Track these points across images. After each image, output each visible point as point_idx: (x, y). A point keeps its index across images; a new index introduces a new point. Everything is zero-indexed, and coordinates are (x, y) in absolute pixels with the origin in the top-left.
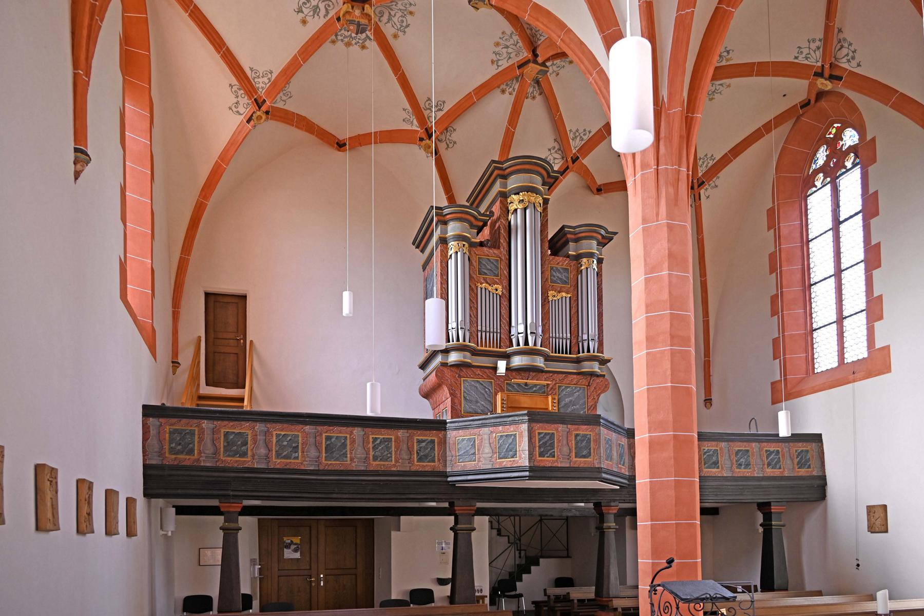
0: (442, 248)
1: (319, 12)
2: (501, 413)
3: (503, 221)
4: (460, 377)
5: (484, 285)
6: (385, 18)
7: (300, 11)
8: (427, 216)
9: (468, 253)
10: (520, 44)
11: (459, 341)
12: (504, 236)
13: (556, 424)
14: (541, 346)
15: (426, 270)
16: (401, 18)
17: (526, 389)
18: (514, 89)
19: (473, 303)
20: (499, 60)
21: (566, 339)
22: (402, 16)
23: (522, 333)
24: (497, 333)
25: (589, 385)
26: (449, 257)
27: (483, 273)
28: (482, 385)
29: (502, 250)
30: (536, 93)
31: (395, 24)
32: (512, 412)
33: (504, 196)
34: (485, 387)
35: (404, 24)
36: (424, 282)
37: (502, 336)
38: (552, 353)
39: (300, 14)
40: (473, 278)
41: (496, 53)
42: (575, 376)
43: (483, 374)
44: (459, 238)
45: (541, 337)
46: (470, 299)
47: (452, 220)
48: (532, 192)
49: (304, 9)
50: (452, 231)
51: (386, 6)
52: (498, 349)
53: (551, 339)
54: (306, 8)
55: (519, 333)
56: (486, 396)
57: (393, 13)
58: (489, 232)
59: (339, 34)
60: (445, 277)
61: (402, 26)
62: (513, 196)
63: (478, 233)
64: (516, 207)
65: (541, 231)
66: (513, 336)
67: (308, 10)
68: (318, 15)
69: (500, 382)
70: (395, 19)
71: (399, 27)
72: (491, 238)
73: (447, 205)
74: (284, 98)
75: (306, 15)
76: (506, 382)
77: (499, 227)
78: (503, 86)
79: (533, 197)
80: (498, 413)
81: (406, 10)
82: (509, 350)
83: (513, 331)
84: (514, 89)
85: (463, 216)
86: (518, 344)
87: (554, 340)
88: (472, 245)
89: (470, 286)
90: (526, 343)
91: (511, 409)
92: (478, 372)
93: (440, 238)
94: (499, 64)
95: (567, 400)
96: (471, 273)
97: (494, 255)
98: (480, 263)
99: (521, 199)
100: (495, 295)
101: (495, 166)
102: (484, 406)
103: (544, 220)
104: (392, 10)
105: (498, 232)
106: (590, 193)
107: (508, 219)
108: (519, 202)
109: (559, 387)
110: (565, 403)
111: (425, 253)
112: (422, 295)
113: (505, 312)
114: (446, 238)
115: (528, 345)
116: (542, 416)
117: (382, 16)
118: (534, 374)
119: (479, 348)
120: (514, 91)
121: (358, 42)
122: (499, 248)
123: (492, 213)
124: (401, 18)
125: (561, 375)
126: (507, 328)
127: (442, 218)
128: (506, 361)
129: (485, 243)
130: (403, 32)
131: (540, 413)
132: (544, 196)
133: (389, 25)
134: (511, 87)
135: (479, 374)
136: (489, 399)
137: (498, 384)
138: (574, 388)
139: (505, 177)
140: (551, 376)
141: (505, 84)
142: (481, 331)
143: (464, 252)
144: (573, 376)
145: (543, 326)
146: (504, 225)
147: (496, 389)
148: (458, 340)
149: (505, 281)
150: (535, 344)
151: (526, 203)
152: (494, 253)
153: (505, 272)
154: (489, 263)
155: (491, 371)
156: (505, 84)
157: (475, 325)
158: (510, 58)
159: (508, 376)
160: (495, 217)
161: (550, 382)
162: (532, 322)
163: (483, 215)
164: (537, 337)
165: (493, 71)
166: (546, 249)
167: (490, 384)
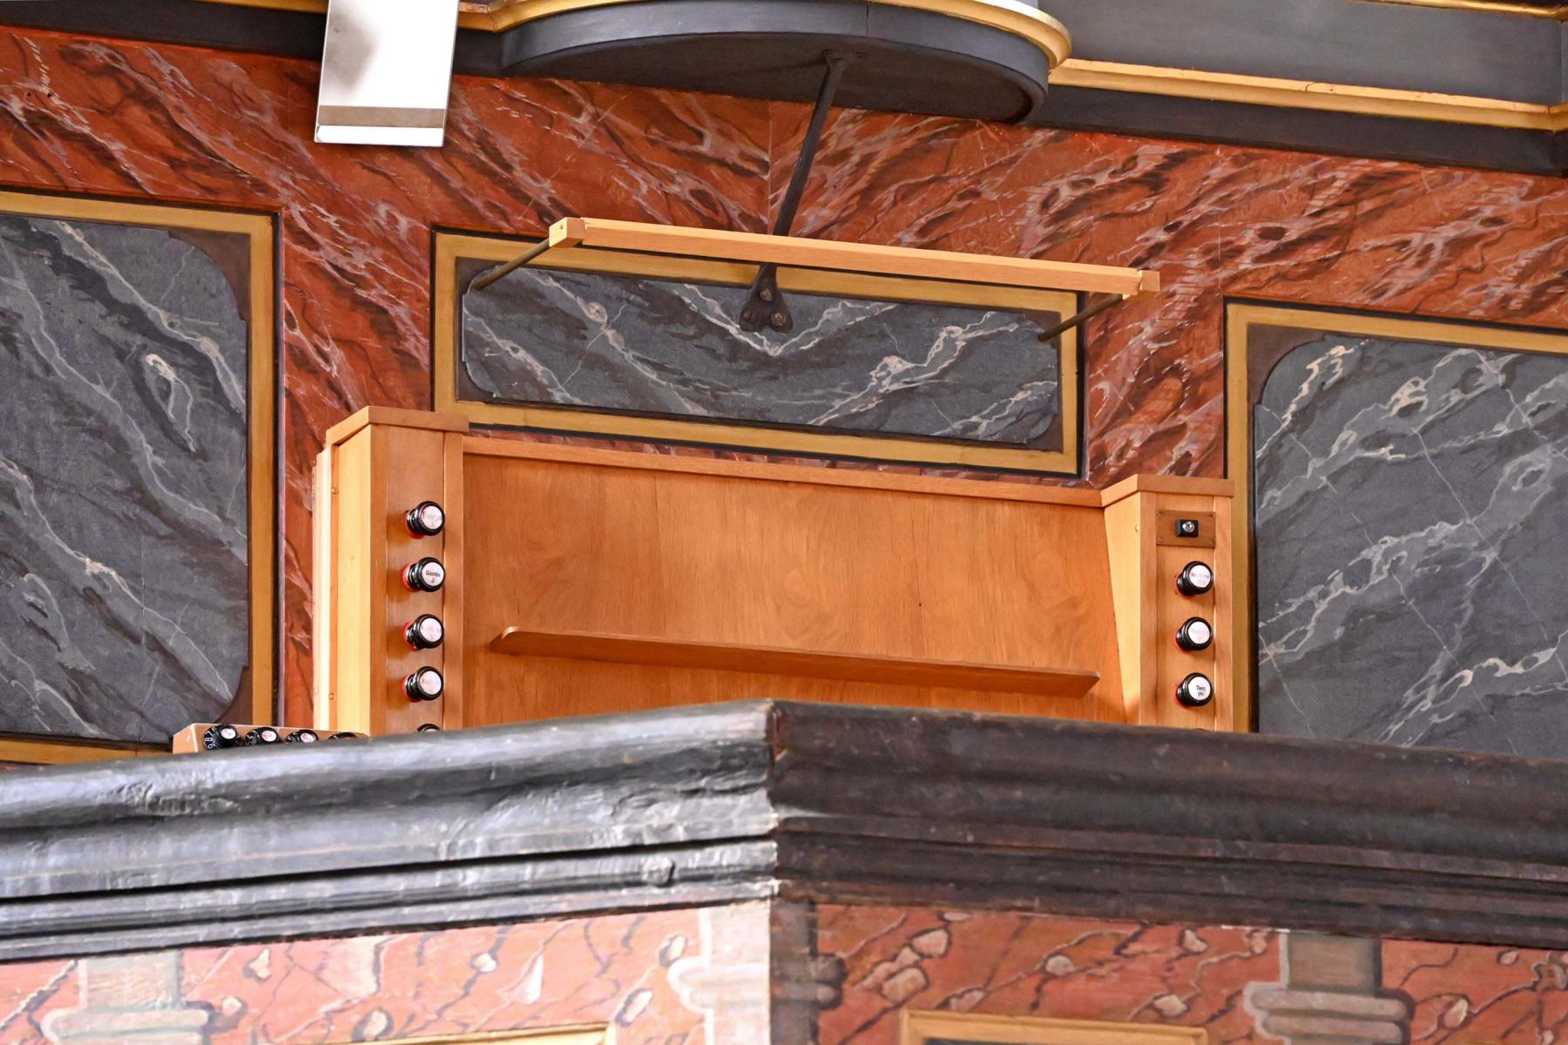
2: (382, 735)
13: (1200, 921)
28: (89, 282)
32: (537, 717)
34: (135, 319)
43: (103, 112)
69: (360, 261)
76: (450, 247)
80: (345, 738)
91: (533, 681)
102: (115, 624)
110: (1355, 615)
116: (990, 795)
125: (1302, 173)
131: (958, 745)
135: (42, 122)
136: (196, 512)
137: (343, 285)
138: (1492, 373)
140: (1154, 182)
144: (1466, 186)
147: (302, 362)
155: (229, 69)
159: (495, 172)
161: (1119, 279)
167: (215, 280)
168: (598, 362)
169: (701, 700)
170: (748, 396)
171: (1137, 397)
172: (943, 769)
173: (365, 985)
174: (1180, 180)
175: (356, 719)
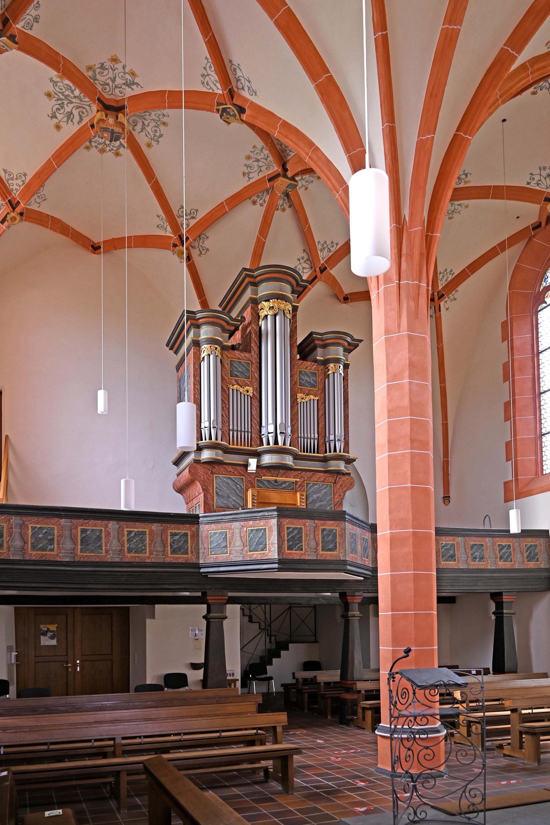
0: (195, 351)
1: (73, 118)
3: (253, 326)
4: (212, 473)
5: (235, 386)
6: (139, 127)
7: (54, 116)
8: (181, 319)
9: (220, 356)
10: (271, 158)
11: (212, 440)
12: (255, 340)
14: (290, 446)
15: (180, 370)
16: (154, 128)
17: (276, 485)
18: (265, 201)
19: (225, 403)
20: (250, 173)
21: (314, 439)
22: (155, 126)
23: (272, 433)
24: (248, 432)
25: (335, 483)
26: (202, 359)
27: (235, 376)
28: (234, 481)
29: (253, 353)
30: (286, 206)
31: (148, 133)
32: (262, 508)
33: (255, 302)
34: (236, 483)
35: (158, 134)
36: (178, 382)
37: (253, 435)
38: (301, 452)
39: (54, 119)
40: (225, 379)
41: (247, 166)
42: (322, 474)
43: (235, 471)
44: (212, 341)
45: (290, 437)
46: (222, 400)
47: (205, 323)
48: (282, 299)
49: (58, 115)
50: (205, 334)
51: (139, 116)
52: (249, 448)
53: (300, 439)
54: (60, 114)
55: (269, 433)
56: (237, 491)
57: (146, 123)
58: (240, 336)
59: (93, 140)
60: (198, 378)
61: (155, 136)
62: (264, 303)
63: (230, 337)
64: (267, 314)
65: (290, 337)
66: (264, 436)
67: (62, 116)
68: (72, 121)
69: (250, 479)
70: (149, 129)
71: (153, 136)
72: (242, 342)
73: (200, 309)
74: (38, 200)
75: (60, 121)
76: (256, 478)
77: (250, 332)
78: (255, 198)
79: (283, 304)
80: (249, 509)
81: (159, 120)
82: (260, 448)
83: (264, 431)
84: (265, 201)
85: (216, 320)
86: (268, 444)
87: (302, 439)
88: (224, 348)
89: (222, 387)
90: (276, 442)
91: (262, 505)
92: (230, 469)
93: (193, 340)
94: (250, 177)
95: (315, 496)
96: (223, 375)
97: (245, 359)
98: (231, 365)
99: (271, 306)
100: (246, 397)
101: (246, 274)
103: (293, 326)
104: (146, 120)
105: (249, 337)
106: (336, 300)
107: (258, 324)
108: (269, 308)
109: (307, 484)
110: (313, 500)
111: (178, 355)
112: (175, 395)
113: (255, 413)
114: (199, 341)
115: (278, 444)
116: (290, 512)
117: (136, 125)
118: (283, 471)
119: (231, 446)
120: (265, 203)
121: (112, 149)
122: (250, 352)
123: (243, 319)
124: (154, 128)
126: (258, 427)
127: (195, 322)
128: (256, 460)
129: (237, 346)
130: (157, 141)
132: (293, 304)
133: (143, 134)
134: (261, 199)
135: (231, 471)
136: (240, 495)
139: (256, 284)
140: (300, 474)
141: (256, 195)
142: (233, 430)
143: (216, 355)
145: (292, 426)
146: (255, 330)
147: (247, 485)
148: (210, 438)
149: (256, 384)
150: (284, 444)
151: (275, 309)
152: (246, 357)
153: (256, 375)
154: (240, 365)
155: (242, 468)
156: (256, 195)
157: (227, 424)
158: (261, 171)
159: (259, 474)
160: (246, 322)
161: (298, 480)
162: (282, 423)
163: (235, 320)
164: (287, 437)
165: (244, 183)
166: (295, 354)
168: (265, 485)
169: (272, 506)
170: (275, 487)
171: (299, 487)
172: (287, 510)
173: (252, 524)
174: (302, 474)
175: (251, 507)
